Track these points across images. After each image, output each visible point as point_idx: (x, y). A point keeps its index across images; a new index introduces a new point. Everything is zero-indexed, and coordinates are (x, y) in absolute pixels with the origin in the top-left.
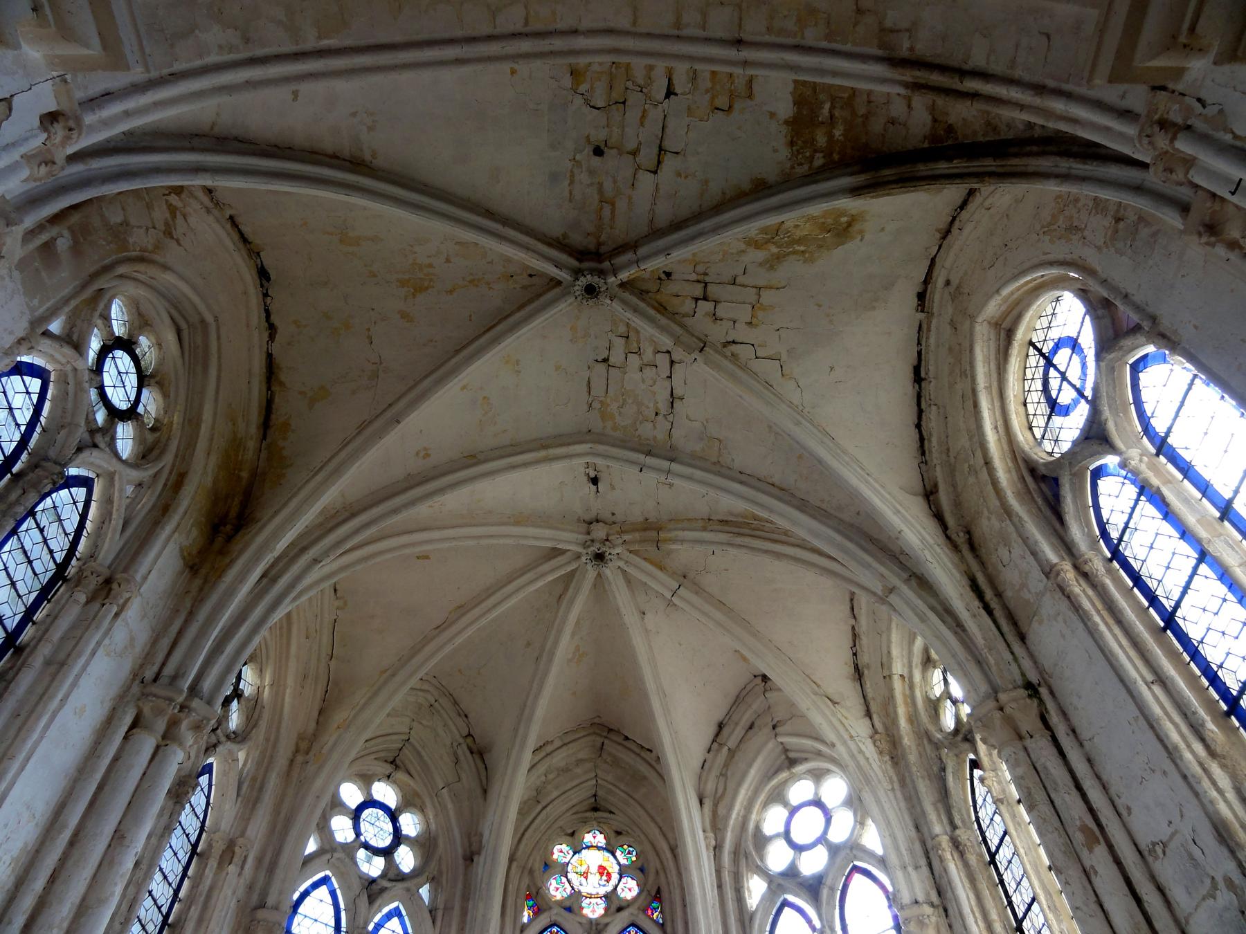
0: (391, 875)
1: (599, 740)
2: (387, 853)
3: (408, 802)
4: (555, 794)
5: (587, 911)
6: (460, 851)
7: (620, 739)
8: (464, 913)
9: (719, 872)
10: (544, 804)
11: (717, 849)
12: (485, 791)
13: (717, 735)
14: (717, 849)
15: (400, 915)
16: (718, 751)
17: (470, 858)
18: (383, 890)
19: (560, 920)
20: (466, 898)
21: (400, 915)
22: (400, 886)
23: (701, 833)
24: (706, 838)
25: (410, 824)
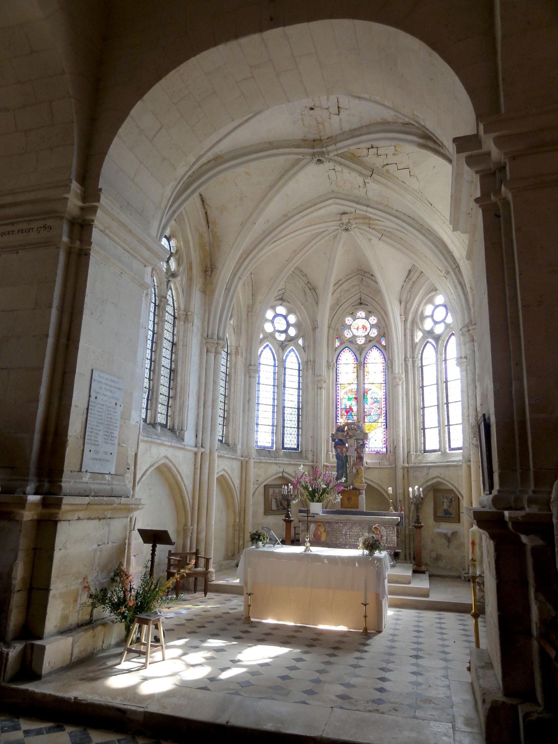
0: (288, 339)
1: (361, 277)
2: (285, 331)
3: (290, 311)
4: (344, 301)
5: (358, 342)
6: (311, 327)
7: (369, 276)
8: (315, 348)
9: (405, 330)
10: (340, 305)
11: (405, 321)
12: (317, 303)
13: (408, 275)
14: (405, 321)
15: (293, 351)
16: (408, 282)
17: (314, 329)
18: (286, 345)
19: (348, 346)
20: (314, 342)
21: (293, 351)
22: (292, 343)
23: (398, 317)
24: (401, 318)
25: (292, 319)
